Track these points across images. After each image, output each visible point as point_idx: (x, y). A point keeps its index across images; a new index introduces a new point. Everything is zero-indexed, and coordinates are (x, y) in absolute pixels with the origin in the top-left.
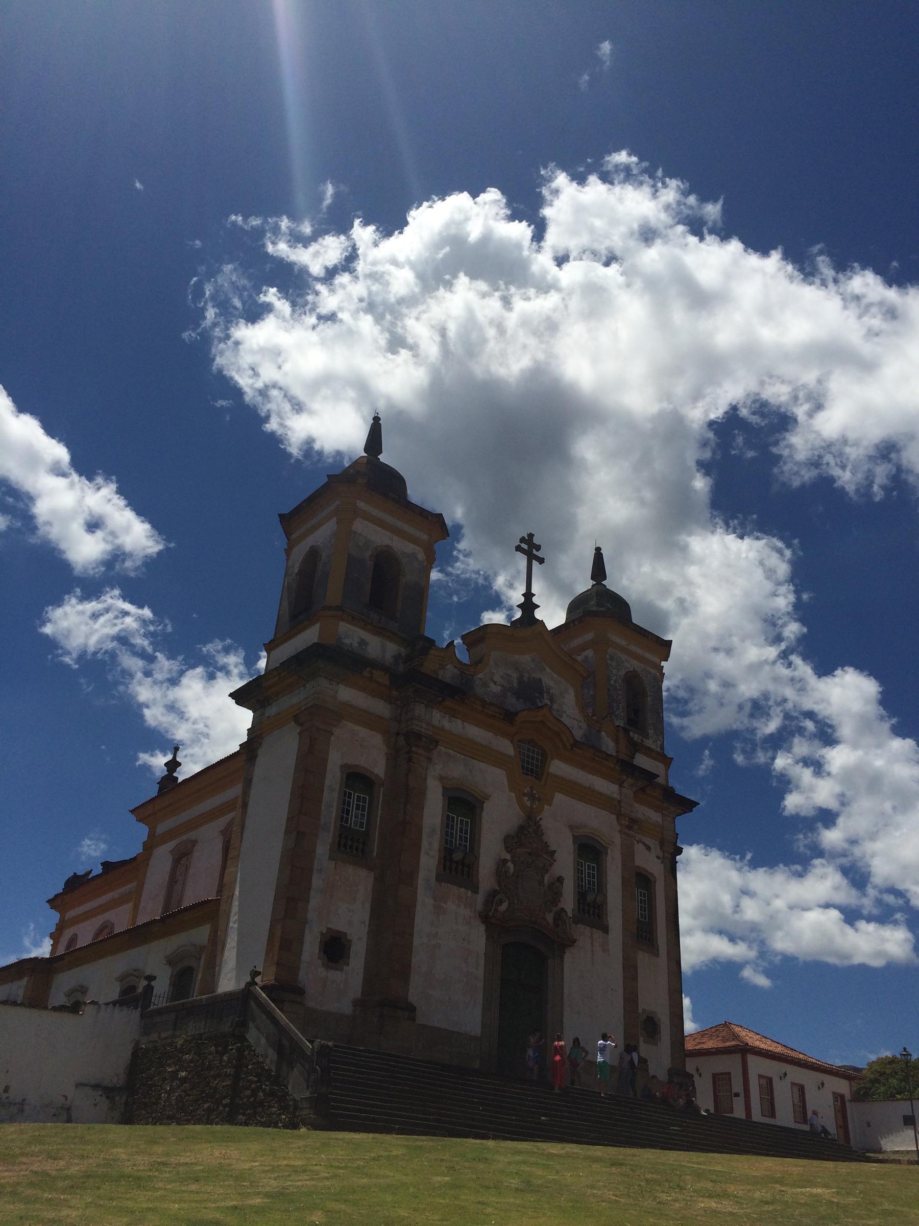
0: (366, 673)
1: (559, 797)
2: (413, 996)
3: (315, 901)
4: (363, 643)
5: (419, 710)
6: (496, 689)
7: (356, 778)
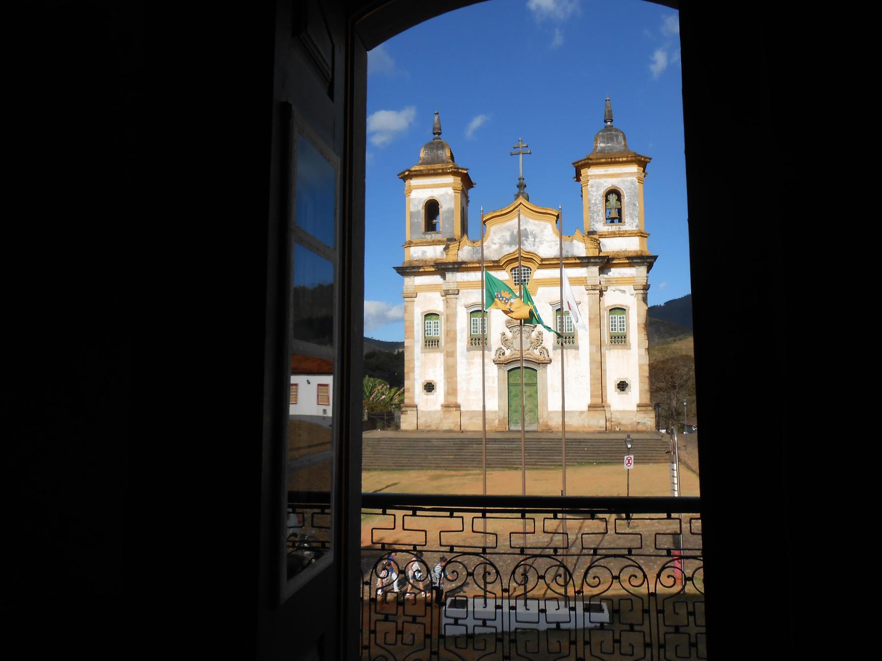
0: (421, 270)
1: (541, 290)
2: (460, 400)
3: (417, 371)
4: (424, 252)
5: (449, 276)
6: (494, 247)
7: (428, 315)
